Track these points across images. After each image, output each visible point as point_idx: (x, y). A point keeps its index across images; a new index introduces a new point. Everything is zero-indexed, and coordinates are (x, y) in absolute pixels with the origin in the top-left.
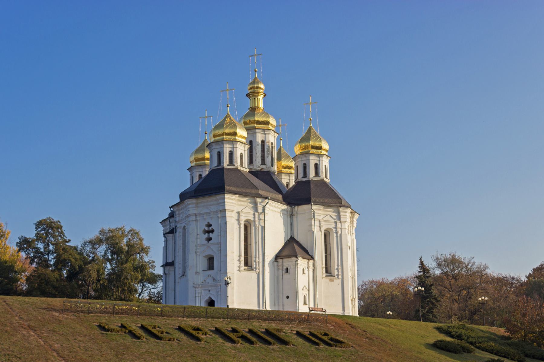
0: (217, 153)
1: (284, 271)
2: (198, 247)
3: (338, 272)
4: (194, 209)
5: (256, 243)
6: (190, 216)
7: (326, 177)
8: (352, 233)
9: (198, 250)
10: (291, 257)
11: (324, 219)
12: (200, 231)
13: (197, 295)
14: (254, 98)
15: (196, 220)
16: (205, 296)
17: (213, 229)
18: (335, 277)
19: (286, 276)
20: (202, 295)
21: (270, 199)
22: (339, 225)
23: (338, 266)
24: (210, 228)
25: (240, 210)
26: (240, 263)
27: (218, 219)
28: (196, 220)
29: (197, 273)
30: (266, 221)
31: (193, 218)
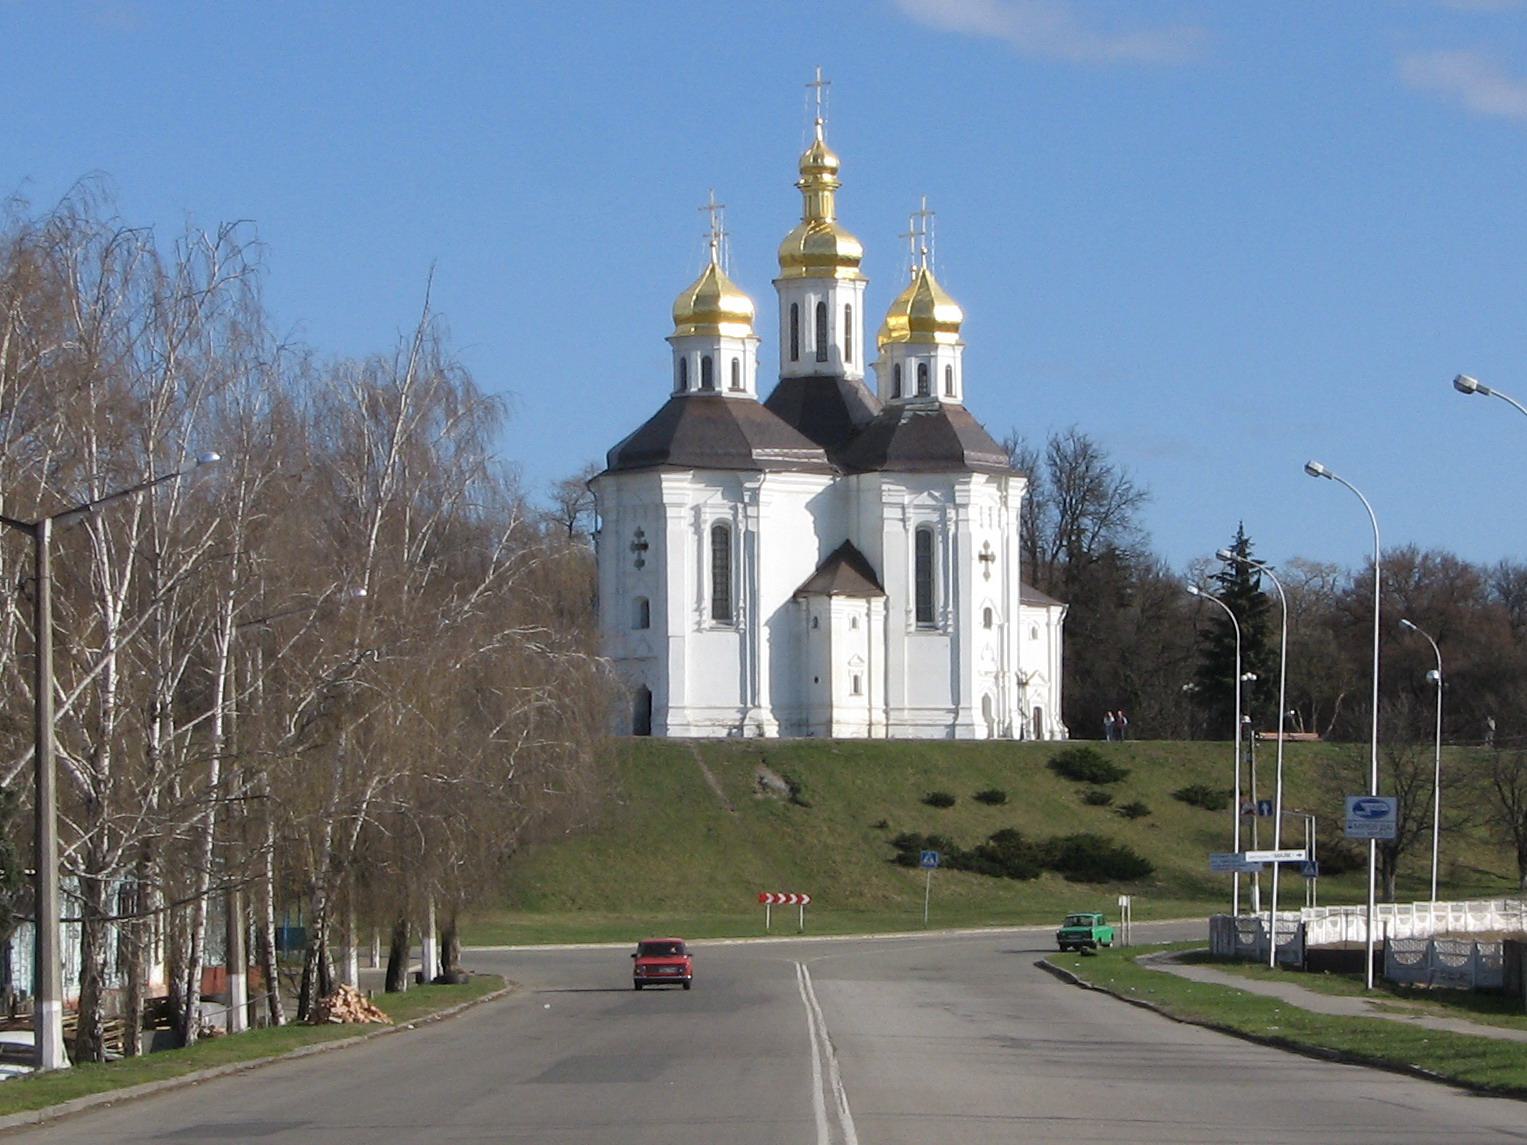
1: (812, 624)
3: (946, 619)
7: (949, 392)
8: (1003, 523)
11: (915, 502)
14: (810, 197)
19: (814, 634)
21: (771, 472)
22: (951, 513)
23: (946, 605)
24: (643, 539)
25: (701, 501)
26: (701, 616)
30: (761, 520)
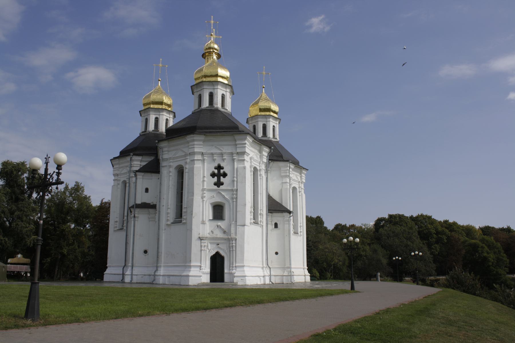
0: (209, 93)
2: (205, 192)
4: (202, 146)
5: (260, 194)
6: (195, 154)
9: (205, 195)
10: (282, 212)
12: (207, 174)
13: (203, 249)
15: (203, 160)
16: (212, 250)
17: (226, 172)
18: (298, 233)
20: (208, 249)
24: (222, 171)
27: (234, 162)
28: (203, 160)
29: (203, 223)
31: (199, 157)
